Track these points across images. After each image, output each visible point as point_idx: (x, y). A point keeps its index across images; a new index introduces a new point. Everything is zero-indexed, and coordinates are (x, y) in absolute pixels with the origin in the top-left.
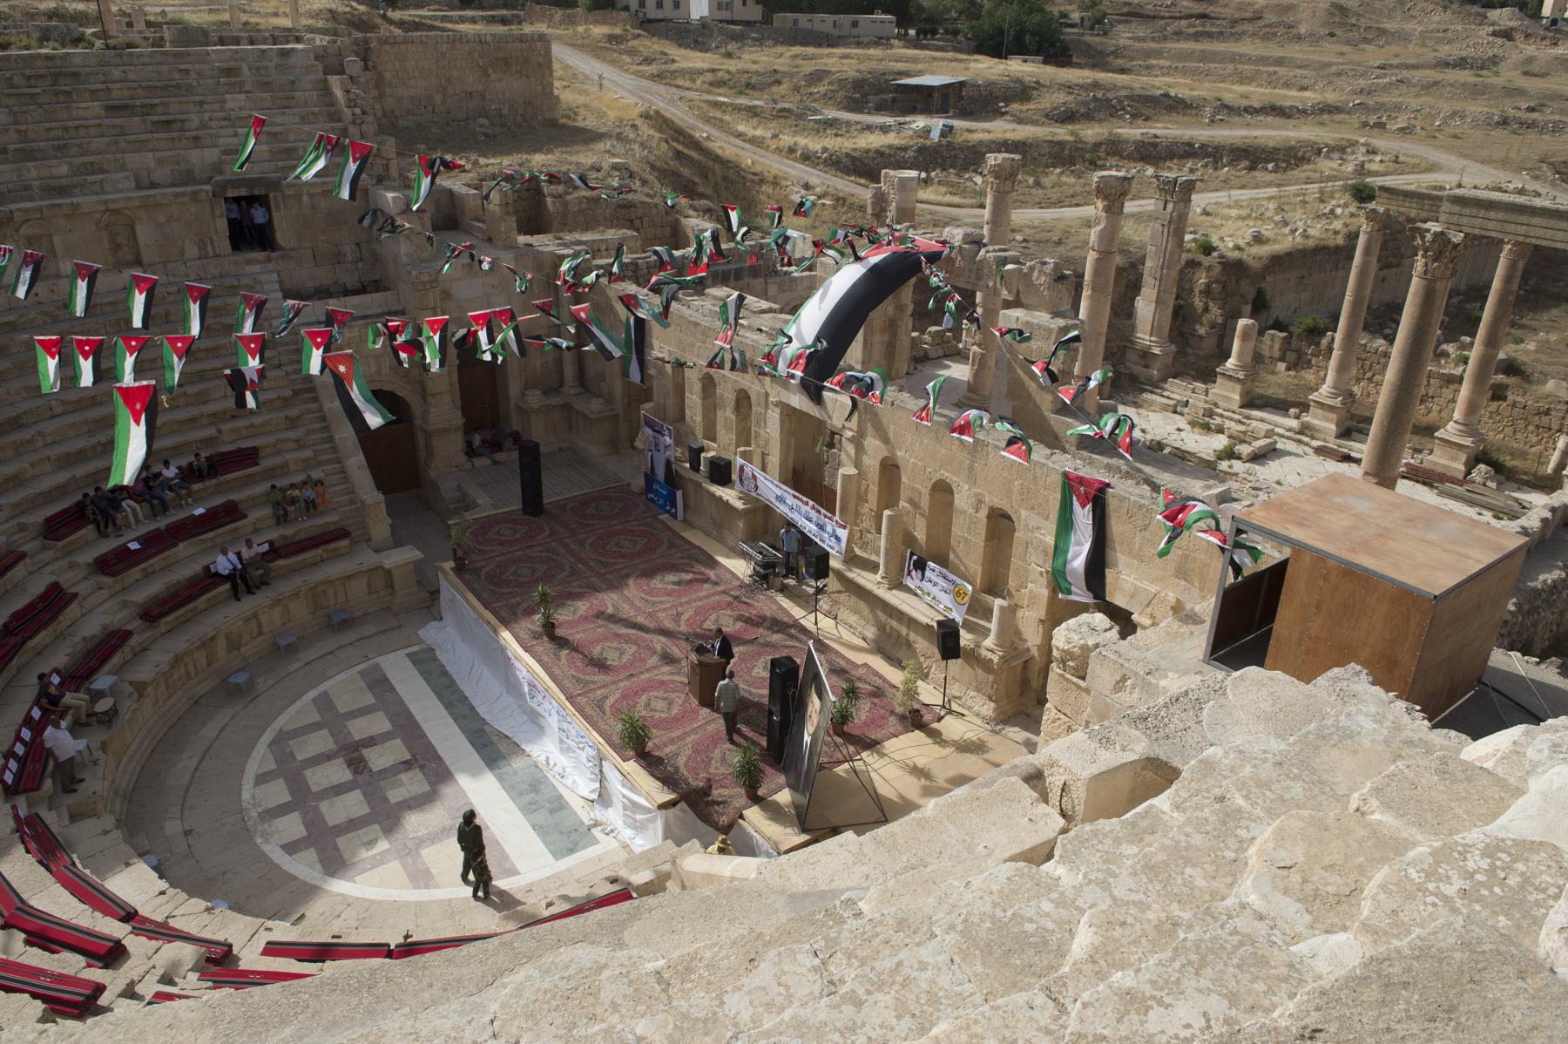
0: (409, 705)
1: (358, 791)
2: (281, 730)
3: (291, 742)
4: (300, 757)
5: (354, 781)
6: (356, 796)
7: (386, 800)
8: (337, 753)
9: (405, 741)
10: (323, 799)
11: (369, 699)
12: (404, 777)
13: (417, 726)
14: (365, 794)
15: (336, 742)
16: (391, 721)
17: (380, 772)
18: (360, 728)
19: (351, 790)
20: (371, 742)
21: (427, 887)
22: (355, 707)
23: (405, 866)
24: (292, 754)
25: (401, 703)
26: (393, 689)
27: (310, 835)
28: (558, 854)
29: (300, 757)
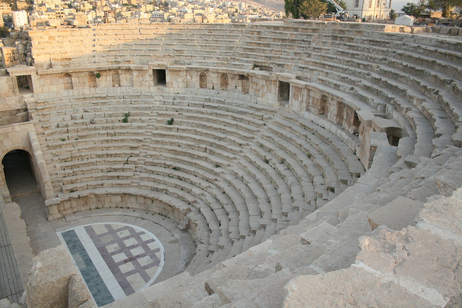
0: (113, 276)
1: (127, 246)
2: (158, 267)
3: (153, 262)
4: (148, 257)
5: (129, 250)
6: (128, 245)
7: (119, 244)
8: (136, 258)
9: (114, 262)
10: (137, 244)
11: (129, 278)
12: (113, 250)
13: (110, 267)
14: (125, 245)
15: (137, 261)
16: (119, 270)
17: (121, 252)
18: (129, 267)
19: (129, 247)
20: (125, 261)
21: (107, 225)
22: (133, 275)
23: (112, 228)
24: (151, 258)
25: (116, 277)
26: (120, 283)
27: (139, 236)
28: (73, 231)
29: (148, 257)
